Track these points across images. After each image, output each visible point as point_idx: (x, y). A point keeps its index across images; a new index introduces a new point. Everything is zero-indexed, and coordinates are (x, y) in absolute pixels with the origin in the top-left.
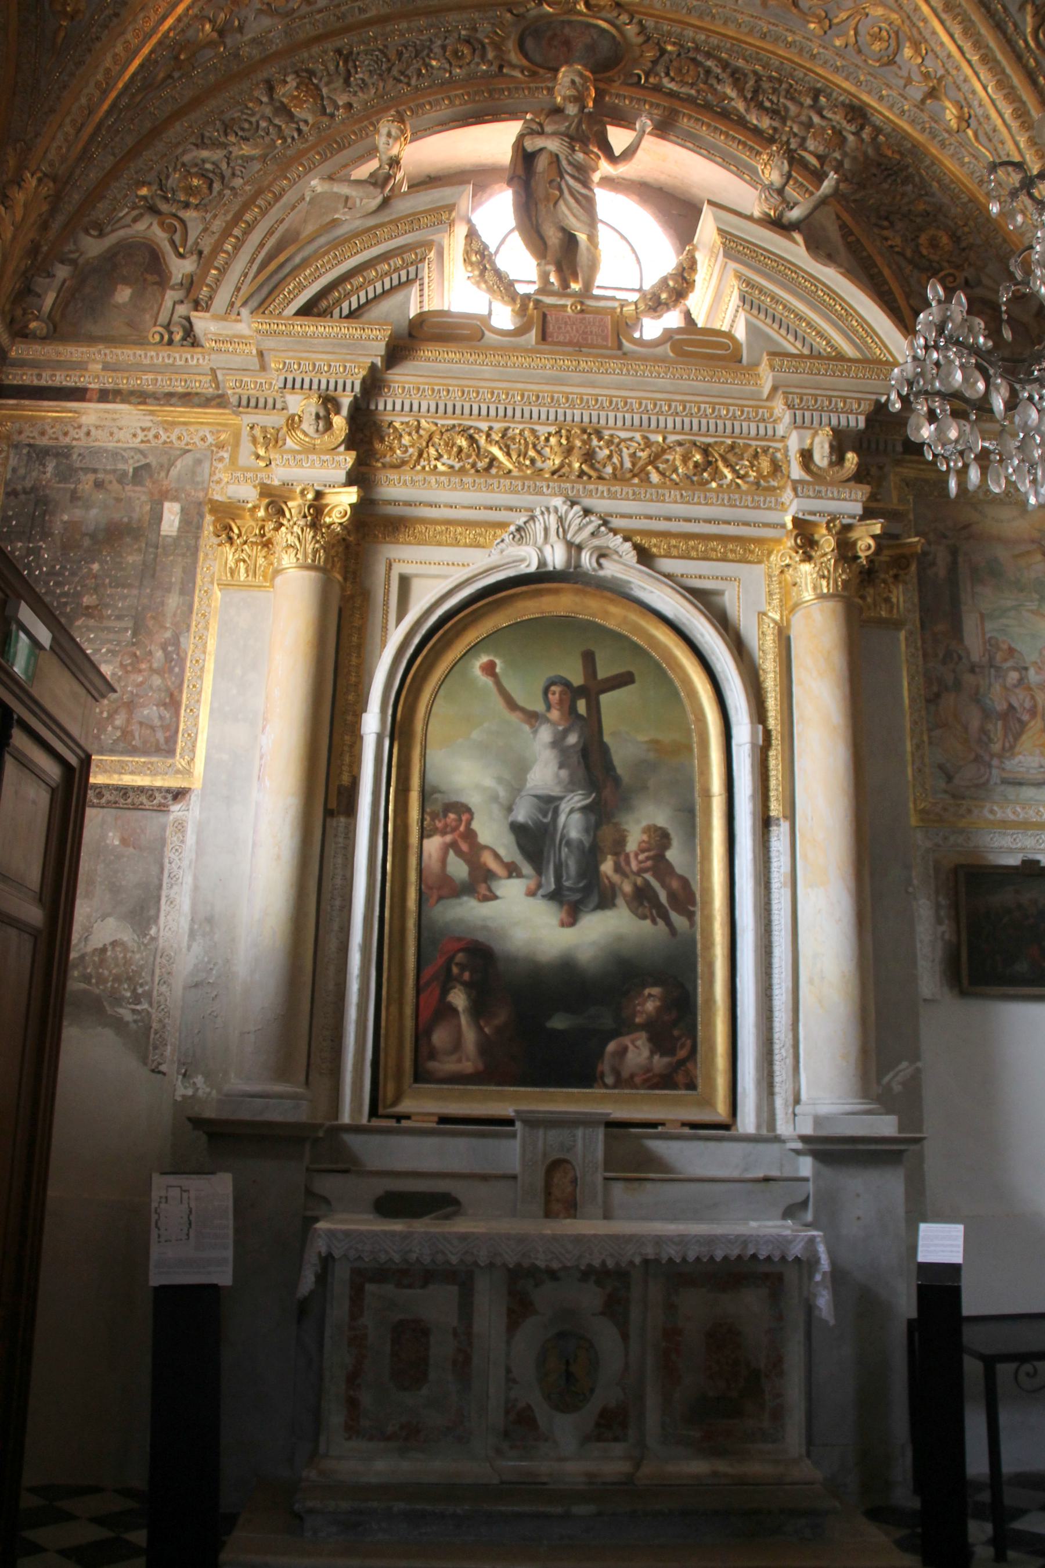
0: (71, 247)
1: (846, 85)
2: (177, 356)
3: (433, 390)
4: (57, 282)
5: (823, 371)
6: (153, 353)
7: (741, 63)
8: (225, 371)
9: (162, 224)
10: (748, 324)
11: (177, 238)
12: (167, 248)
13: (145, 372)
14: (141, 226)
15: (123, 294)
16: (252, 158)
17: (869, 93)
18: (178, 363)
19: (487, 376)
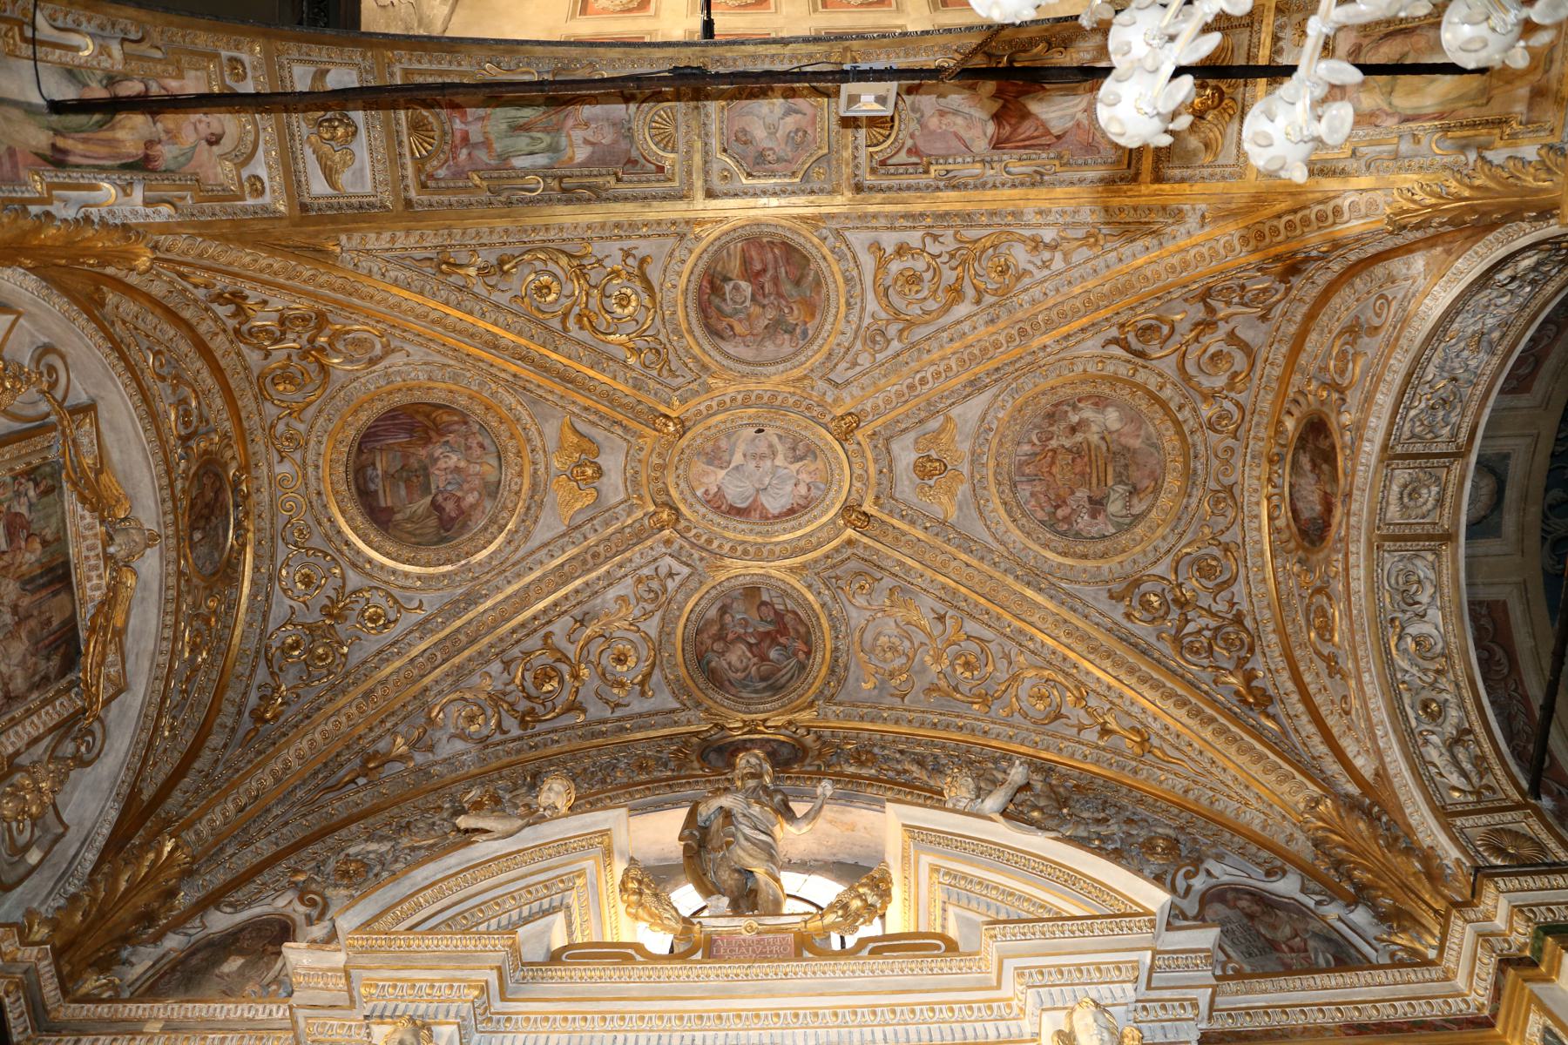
0: (197, 922)
1: (1023, 749)
2: (261, 1008)
3: (566, 1019)
4: (159, 951)
5: (1058, 934)
6: (232, 1006)
7: (919, 750)
8: (308, 1012)
9: (301, 900)
10: (958, 917)
11: (315, 913)
12: (300, 919)
13: (214, 1030)
14: (281, 903)
15: (234, 964)
16: (420, 848)
17: (1047, 749)
18: (260, 1016)
19: (635, 994)
